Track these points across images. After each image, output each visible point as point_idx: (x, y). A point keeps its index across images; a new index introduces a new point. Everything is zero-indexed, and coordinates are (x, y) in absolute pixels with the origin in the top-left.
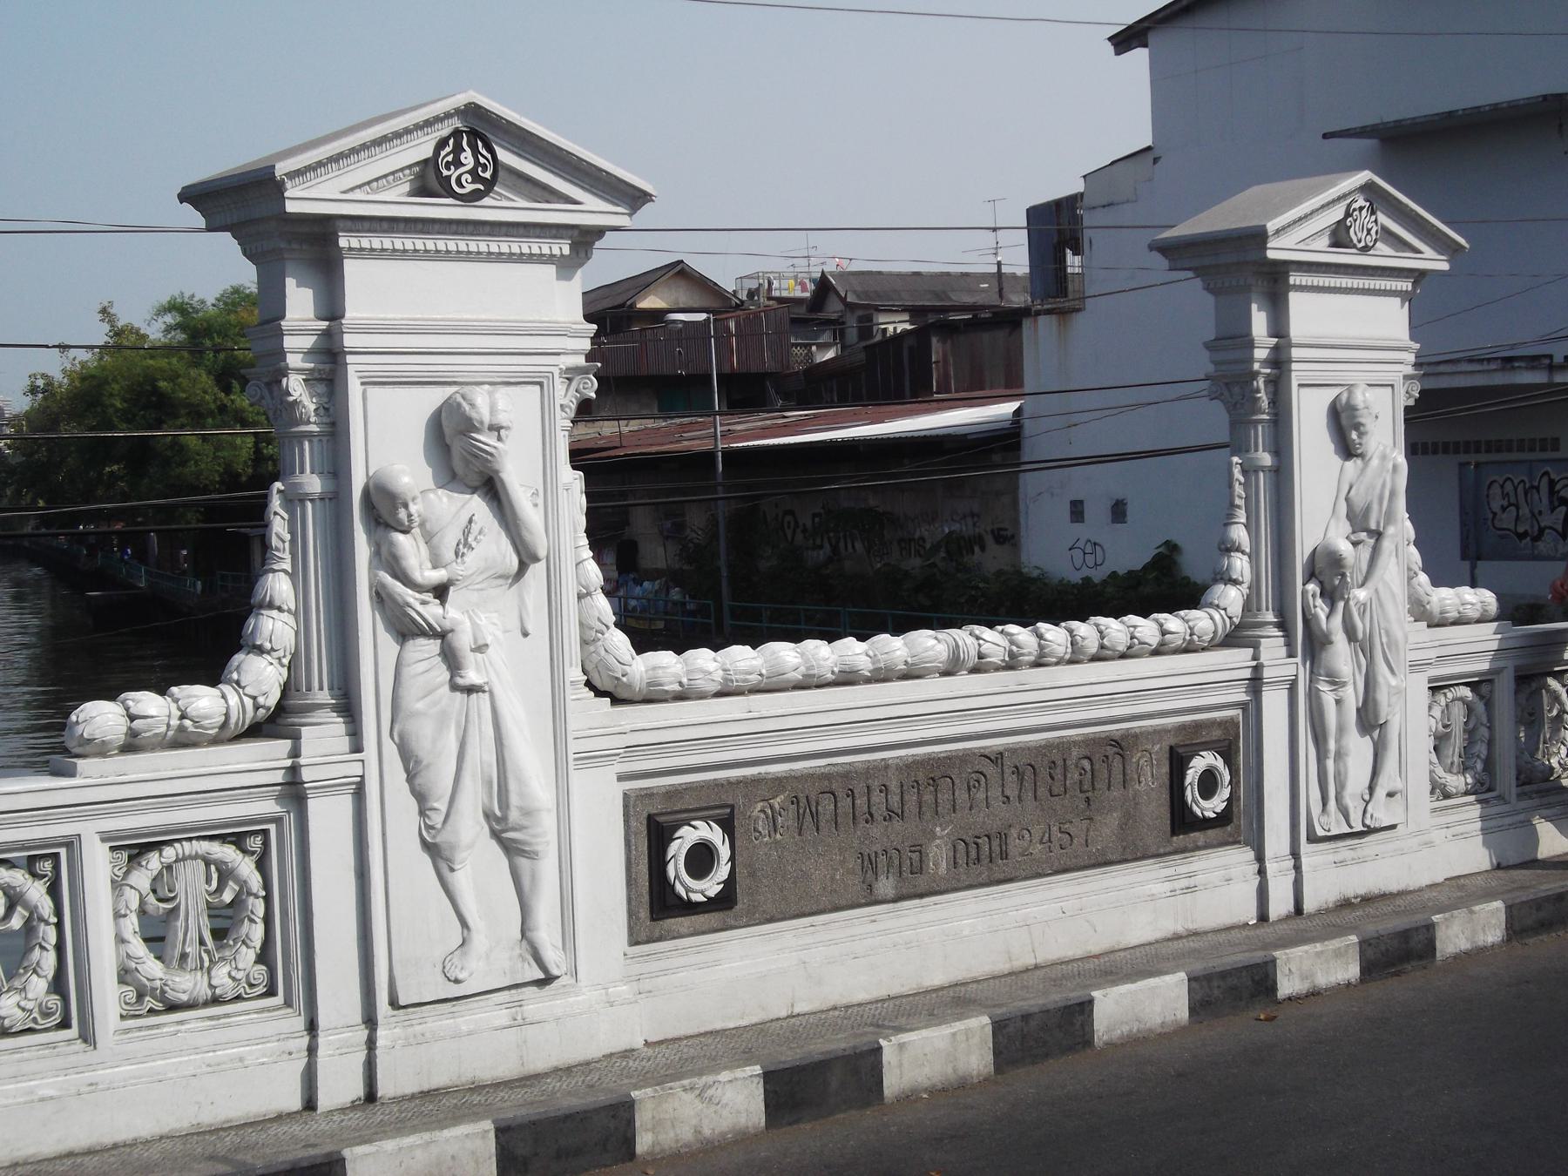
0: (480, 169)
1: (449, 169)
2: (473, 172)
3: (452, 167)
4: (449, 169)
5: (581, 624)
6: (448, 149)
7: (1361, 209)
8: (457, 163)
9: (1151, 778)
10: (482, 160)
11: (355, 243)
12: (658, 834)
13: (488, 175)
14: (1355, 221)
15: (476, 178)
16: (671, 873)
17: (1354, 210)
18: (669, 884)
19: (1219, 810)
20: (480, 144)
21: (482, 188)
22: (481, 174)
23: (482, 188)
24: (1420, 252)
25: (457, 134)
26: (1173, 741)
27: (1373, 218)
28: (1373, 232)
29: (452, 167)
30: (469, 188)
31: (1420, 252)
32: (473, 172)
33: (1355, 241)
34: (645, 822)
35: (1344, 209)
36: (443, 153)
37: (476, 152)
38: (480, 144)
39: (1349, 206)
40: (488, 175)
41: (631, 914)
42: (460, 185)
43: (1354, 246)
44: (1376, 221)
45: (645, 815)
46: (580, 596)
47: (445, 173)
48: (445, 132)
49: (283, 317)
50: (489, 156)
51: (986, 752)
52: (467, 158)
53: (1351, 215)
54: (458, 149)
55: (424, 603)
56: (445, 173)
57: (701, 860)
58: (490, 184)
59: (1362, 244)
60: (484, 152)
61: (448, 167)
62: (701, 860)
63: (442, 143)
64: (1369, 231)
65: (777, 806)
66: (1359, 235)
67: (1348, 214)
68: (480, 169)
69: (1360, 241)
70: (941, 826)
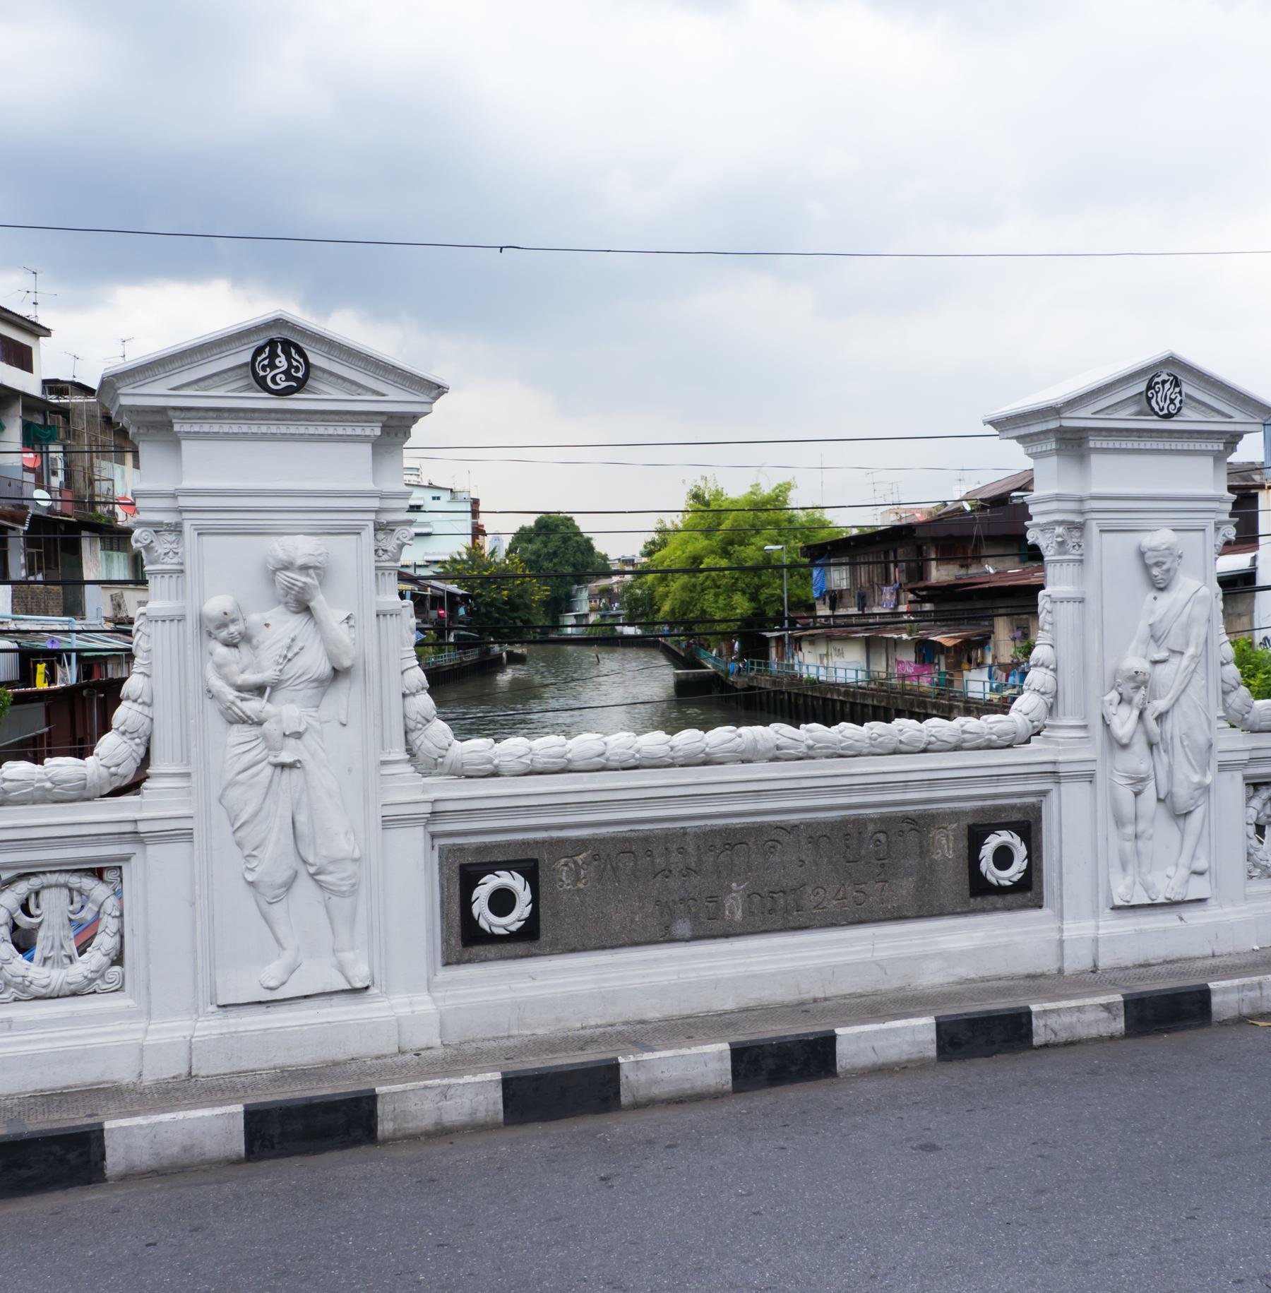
0: (293, 370)
1: (265, 371)
2: (287, 373)
3: (268, 369)
4: (265, 371)
5: (405, 716)
6: (264, 356)
7: (1164, 382)
8: (273, 366)
9: (947, 847)
10: (295, 363)
11: (187, 428)
12: (469, 877)
13: (300, 375)
14: (1157, 393)
16: (475, 911)
17: (1157, 383)
18: (474, 918)
19: (1015, 879)
20: (293, 351)
21: (295, 384)
22: (294, 374)
23: (295, 384)
25: (272, 343)
26: (971, 821)
27: (1177, 390)
28: (1177, 402)
29: (268, 369)
30: (284, 385)
31: (1231, 417)
32: (287, 373)
33: (1157, 408)
34: (457, 871)
35: (1147, 382)
36: (259, 359)
37: (289, 358)
38: (293, 351)
39: (1152, 379)
40: (300, 375)
41: (445, 941)
42: (276, 384)
43: (1157, 414)
44: (1180, 393)
45: (457, 864)
46: (404, 696)
47: (262, 373)
48: (261, 343)
50: (301, 360)
51: (783, 824)
52: (282, 362)
53: (1154, 388)
54: (273, 356)
55: (243, 700)
56: (262, 373)
57: (502, 901)
59: (1165, 411)
60: (297, 357)
61: (264, 368)
62: (502, 901)
63: (259, 351)
64: (1172, 401)
65: (580, 862)
66: (1161, 404)
67: (1149, 387)
68: (293, 370)
69: (1162, 410)
70: (737, 882)
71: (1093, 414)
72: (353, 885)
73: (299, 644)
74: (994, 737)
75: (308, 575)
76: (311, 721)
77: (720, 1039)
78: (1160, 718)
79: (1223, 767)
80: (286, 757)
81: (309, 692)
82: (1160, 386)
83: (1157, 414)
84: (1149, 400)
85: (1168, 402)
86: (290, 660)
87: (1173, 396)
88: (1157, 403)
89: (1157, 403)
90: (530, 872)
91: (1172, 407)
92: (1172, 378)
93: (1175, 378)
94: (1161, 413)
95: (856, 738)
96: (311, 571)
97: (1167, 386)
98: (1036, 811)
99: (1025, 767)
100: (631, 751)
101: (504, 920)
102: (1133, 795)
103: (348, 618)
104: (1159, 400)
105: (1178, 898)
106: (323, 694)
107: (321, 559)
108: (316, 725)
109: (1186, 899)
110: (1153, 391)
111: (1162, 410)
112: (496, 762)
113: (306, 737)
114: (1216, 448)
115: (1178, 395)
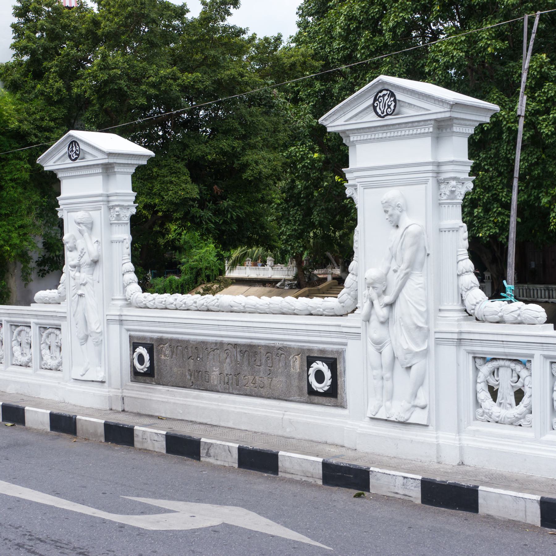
2: (75, 152)
8: (72, 151)
14: (380, 102)
15: (76, 154)
17: (380, 97)
24: (429, 110)
27: (392, 99)
30: (75, 157)
33: (380, 112)
37: (76, 147)
49: (59, 194)
51: (231, 343)
52: (74, 149)
53: (378, 100)
54: (72, 147)
58: (78, 155)
59: (385, 113)
64: (389, 106)
66: (382, 110)
67: (375, 100)
69: (383, 113)
71: (346, 121)
72: (97, 342)
73: (85, 251)
74: (321, 310)
75: (80, 226)
76: (89, 280)
77: (237, 443)
78: (391, 305)
79: (439, 341)
80: (80, 292)
81: (88, 269)
82: (382, 98)
83: (380, 116)
84: (375, 108)
85: (386, 107)
86: (82, 257)
87: (390, 103)
88: (380, 109)
89: (380, 109)
90: (150, 349)
91: (389, 110)
92: (388, 92)
93: (390, 91)
94: (382, 115)
95: (261, 304)
96: (81, 225)
97: (386, 97)
98: (341, 353)
99: (450, 334)
100: (181, 303)
101: (143, 367)
102: (379, 354)
103: (97, 241)
104: (381, 107)
105: (402, 420)
106: (94, 270)
107: (84, 220)
108: (91, 281)
109: (408, 421)
110: (377, 102)
111: (383, 113)
112: (144, 302)
113: (87, 285)
114: (427, 130)
115: (393, 102)
